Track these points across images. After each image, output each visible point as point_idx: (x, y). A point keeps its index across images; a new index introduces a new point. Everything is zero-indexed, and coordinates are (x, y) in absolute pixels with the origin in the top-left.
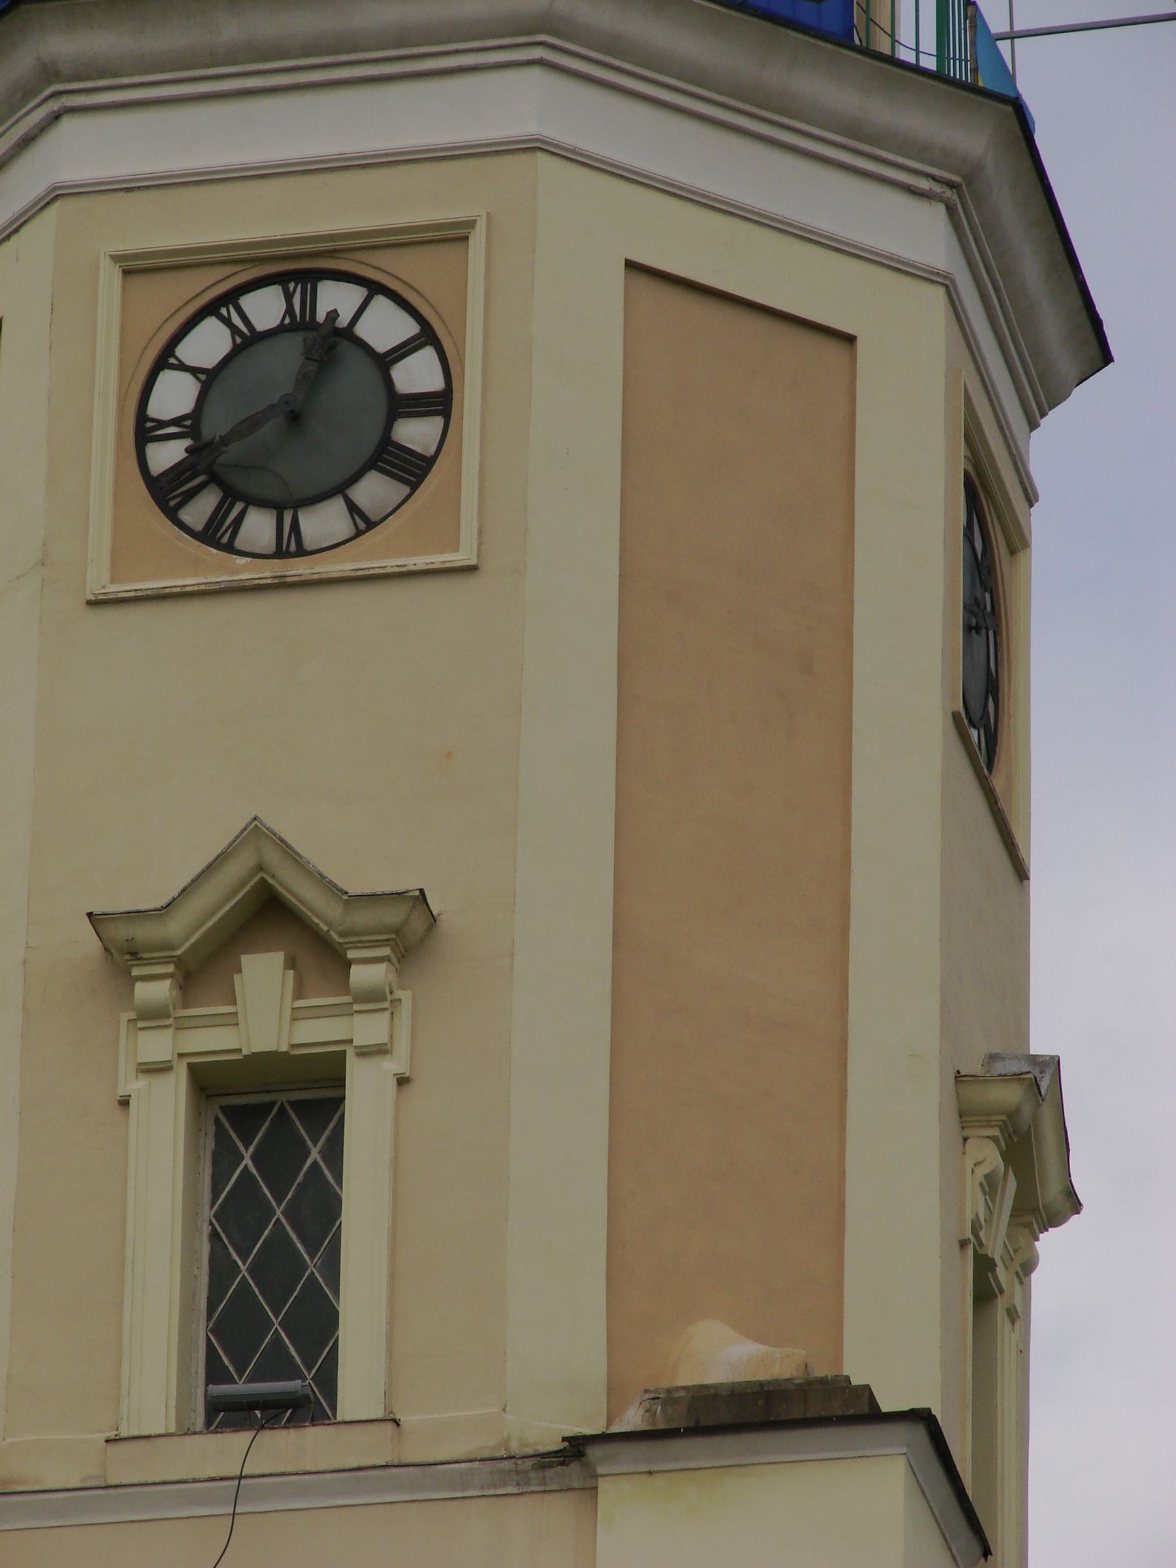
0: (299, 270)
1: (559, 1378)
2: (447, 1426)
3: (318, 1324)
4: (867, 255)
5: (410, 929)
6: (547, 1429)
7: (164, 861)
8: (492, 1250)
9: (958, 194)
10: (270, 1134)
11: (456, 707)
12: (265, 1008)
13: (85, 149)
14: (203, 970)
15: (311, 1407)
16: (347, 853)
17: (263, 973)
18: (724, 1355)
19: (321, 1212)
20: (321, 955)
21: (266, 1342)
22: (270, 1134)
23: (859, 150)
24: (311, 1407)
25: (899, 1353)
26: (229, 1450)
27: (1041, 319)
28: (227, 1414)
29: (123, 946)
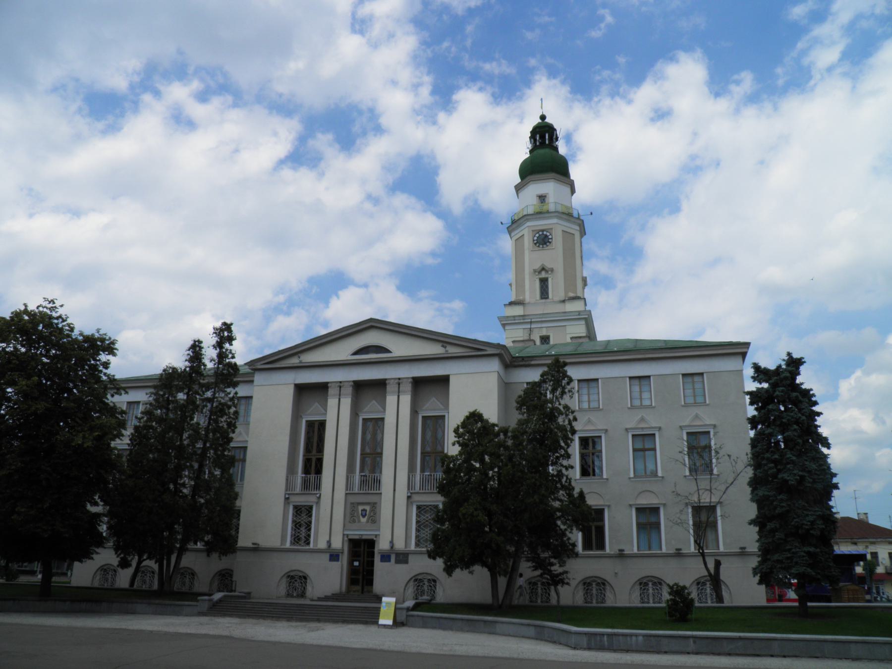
0: (543, 231)
1: (561, 295)
2: (557, 299)
3: (547, 293)
4: (574, 229)
5: (552, 270)
6: (562, 299)
7: (537, 266)
8: (557, 288)
9: (579, 225)
10: (544, 282)
11: (553, 257)
12: (543, 275)
13: (529, 224)
14: (540, 272)
15: (547, 298)
16: (548, 265)
17: (543, 273)
18: (571, 295)
19: (547, 287)
20: (547, 271)
21: (544, 294)
22: (544, 282)
23: (574, 223)
24: (547, 298)
25: (579, 294)
26: (544, 301)
27: (583, 233)
28: (542, 298)
29: (535, 271)
